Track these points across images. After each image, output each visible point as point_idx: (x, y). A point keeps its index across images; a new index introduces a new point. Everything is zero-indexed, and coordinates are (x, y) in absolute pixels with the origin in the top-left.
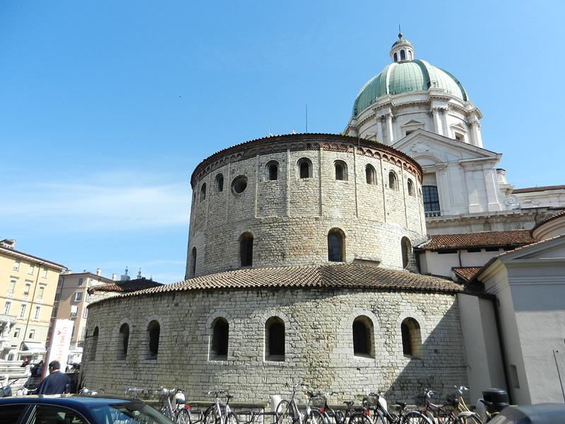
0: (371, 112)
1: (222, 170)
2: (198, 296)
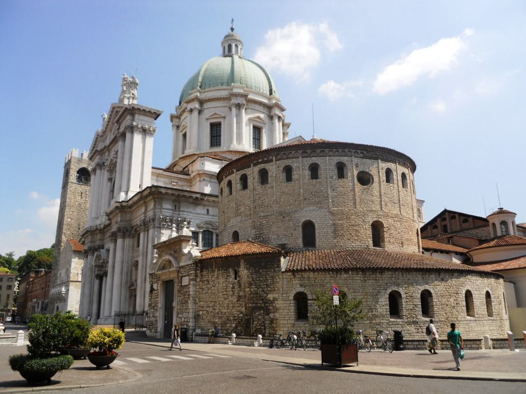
0: (224, 94)
1: (345, 159)
2: (455, 274)
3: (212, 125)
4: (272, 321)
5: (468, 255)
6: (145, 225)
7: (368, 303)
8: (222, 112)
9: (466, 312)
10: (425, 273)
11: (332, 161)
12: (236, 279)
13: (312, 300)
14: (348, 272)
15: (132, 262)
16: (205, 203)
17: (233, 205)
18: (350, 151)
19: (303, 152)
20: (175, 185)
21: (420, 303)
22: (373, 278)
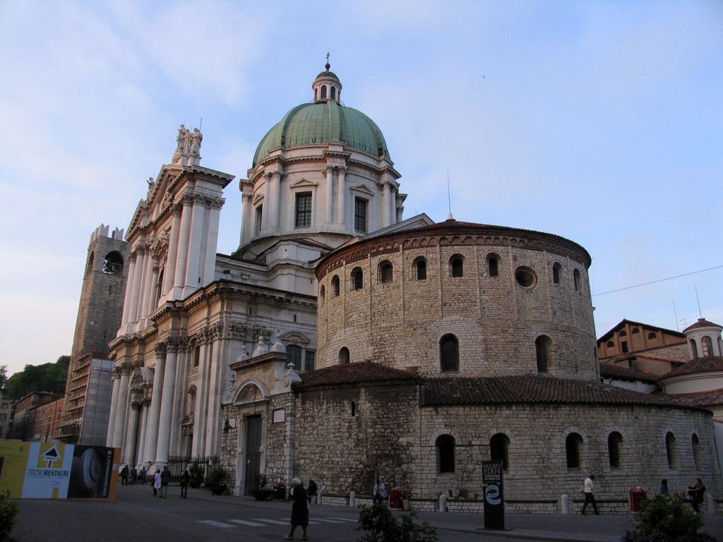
0: (318, 153)
1: (498, 250)
3: (299, 196)
4: (405, 475)
5: (659, 383)
6: (207, 335)
7: (538, 450)
8: (313, 177)
9: (667, 463)
10: (613, 409)
11: (481, 252)
12: (353, 415)
13: (462, 446)
14: (511, 407)
15: (186, 387)
16: (294, 307)
17: (341, 310)
18: (507, 239)
19: (441, 240)
20: (246, 279)
21: (608, 451)
22: (544, 415)
